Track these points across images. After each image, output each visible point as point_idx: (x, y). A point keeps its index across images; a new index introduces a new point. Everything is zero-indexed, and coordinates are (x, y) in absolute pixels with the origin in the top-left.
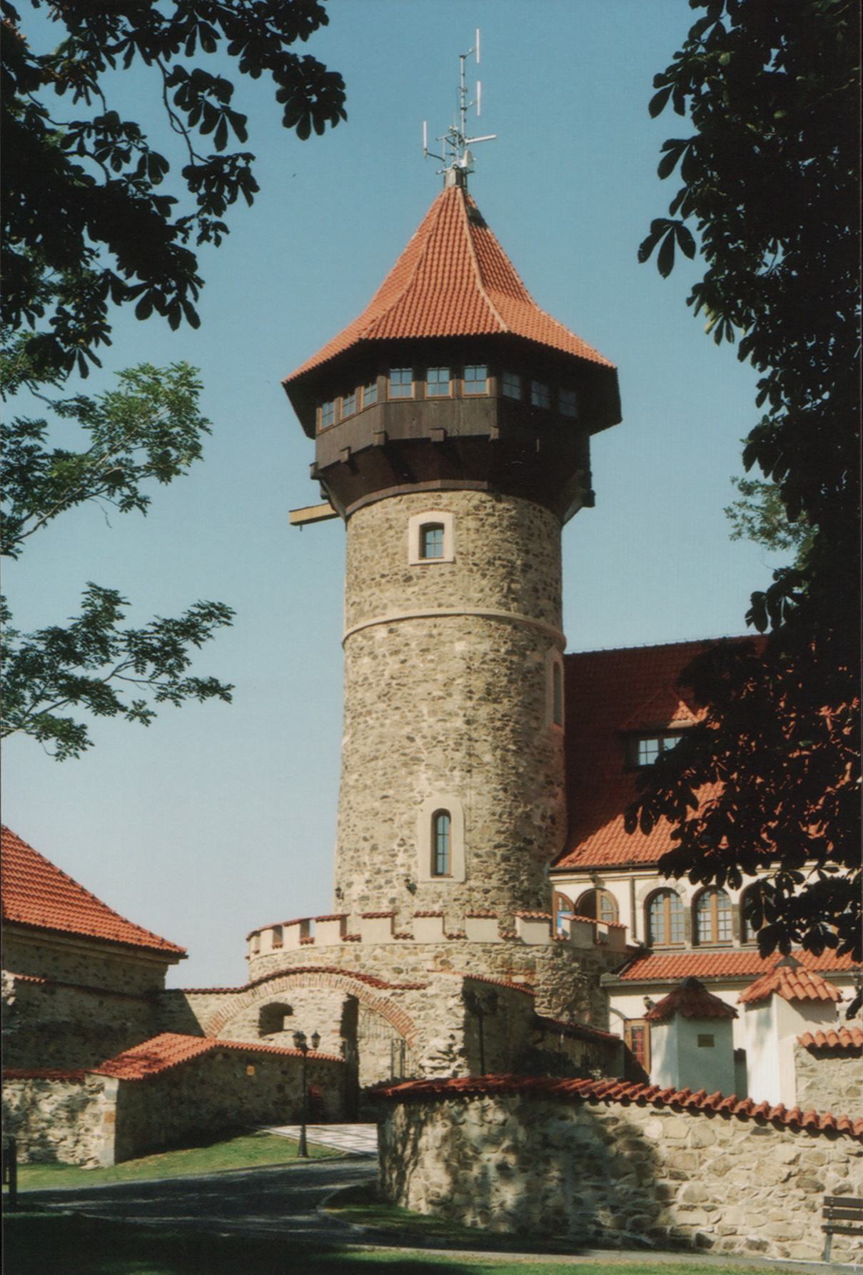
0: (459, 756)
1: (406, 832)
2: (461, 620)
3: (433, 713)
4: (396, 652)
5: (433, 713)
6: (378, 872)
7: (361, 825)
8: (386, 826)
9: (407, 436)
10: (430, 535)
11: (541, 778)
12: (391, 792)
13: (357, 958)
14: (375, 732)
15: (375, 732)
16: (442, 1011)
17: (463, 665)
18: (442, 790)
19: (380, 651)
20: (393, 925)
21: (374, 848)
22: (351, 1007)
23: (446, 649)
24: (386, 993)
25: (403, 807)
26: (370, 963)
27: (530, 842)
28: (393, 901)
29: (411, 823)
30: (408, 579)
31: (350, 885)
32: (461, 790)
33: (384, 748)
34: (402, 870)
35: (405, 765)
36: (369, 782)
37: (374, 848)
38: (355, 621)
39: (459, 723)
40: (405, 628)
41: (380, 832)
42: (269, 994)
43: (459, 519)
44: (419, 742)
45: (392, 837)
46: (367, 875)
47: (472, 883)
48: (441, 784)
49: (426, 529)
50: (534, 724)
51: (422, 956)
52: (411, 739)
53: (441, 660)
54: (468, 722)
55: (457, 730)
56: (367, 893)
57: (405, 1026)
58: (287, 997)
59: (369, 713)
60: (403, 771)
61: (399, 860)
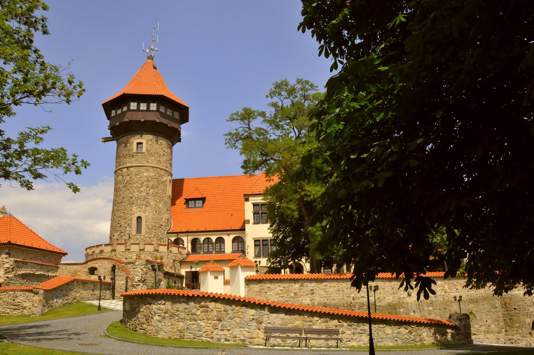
0: (144, 202)
1: (129, 222)
2: (146, 168)
3: (138, 191)
4: (129, 175)
5: (138, 191)
7: (118, 220)
9: (134, 119)
10: (139, 146)
11: (165, 209)
13: (115, 255)
14: (122, 196)
15: (122, 196)
16: (139, 269)
17: (146, 179)
18: (139, 211)
19: (124, 175)
20: (126, 246)
21: (121, 226)
22: (114, 268)
23: (141, 175)
24: (124, 265)
25: (129, 215)
26: (119, 256)
27: (161, 225)
28: (125, 240)
29: (131, 220)
30: (133, 156)
31: (114, 236)
32: (145, 211)
33: (124, 200)
34: (128, 232)
35: (130, 204)
38: (118, 166)
39: (144, 194)
40: (132, 169)
41: (123, 222)
42: (91, 265)
43: (147, 142)
44: (134, 199)
45: (126, 223)
46: (119, 233)
47: (146, 236)
48: (139, 209)
49: (138, 144)
50: (164, 195)
51: (133, 255)
52: (132, 198)
53: (141, 177)
54: (147, 194)
55: (144, 196)
57: (128, 273)
58: (96, 266)
59: (121, 191)
60: (129, 206)
61: (127, 229)
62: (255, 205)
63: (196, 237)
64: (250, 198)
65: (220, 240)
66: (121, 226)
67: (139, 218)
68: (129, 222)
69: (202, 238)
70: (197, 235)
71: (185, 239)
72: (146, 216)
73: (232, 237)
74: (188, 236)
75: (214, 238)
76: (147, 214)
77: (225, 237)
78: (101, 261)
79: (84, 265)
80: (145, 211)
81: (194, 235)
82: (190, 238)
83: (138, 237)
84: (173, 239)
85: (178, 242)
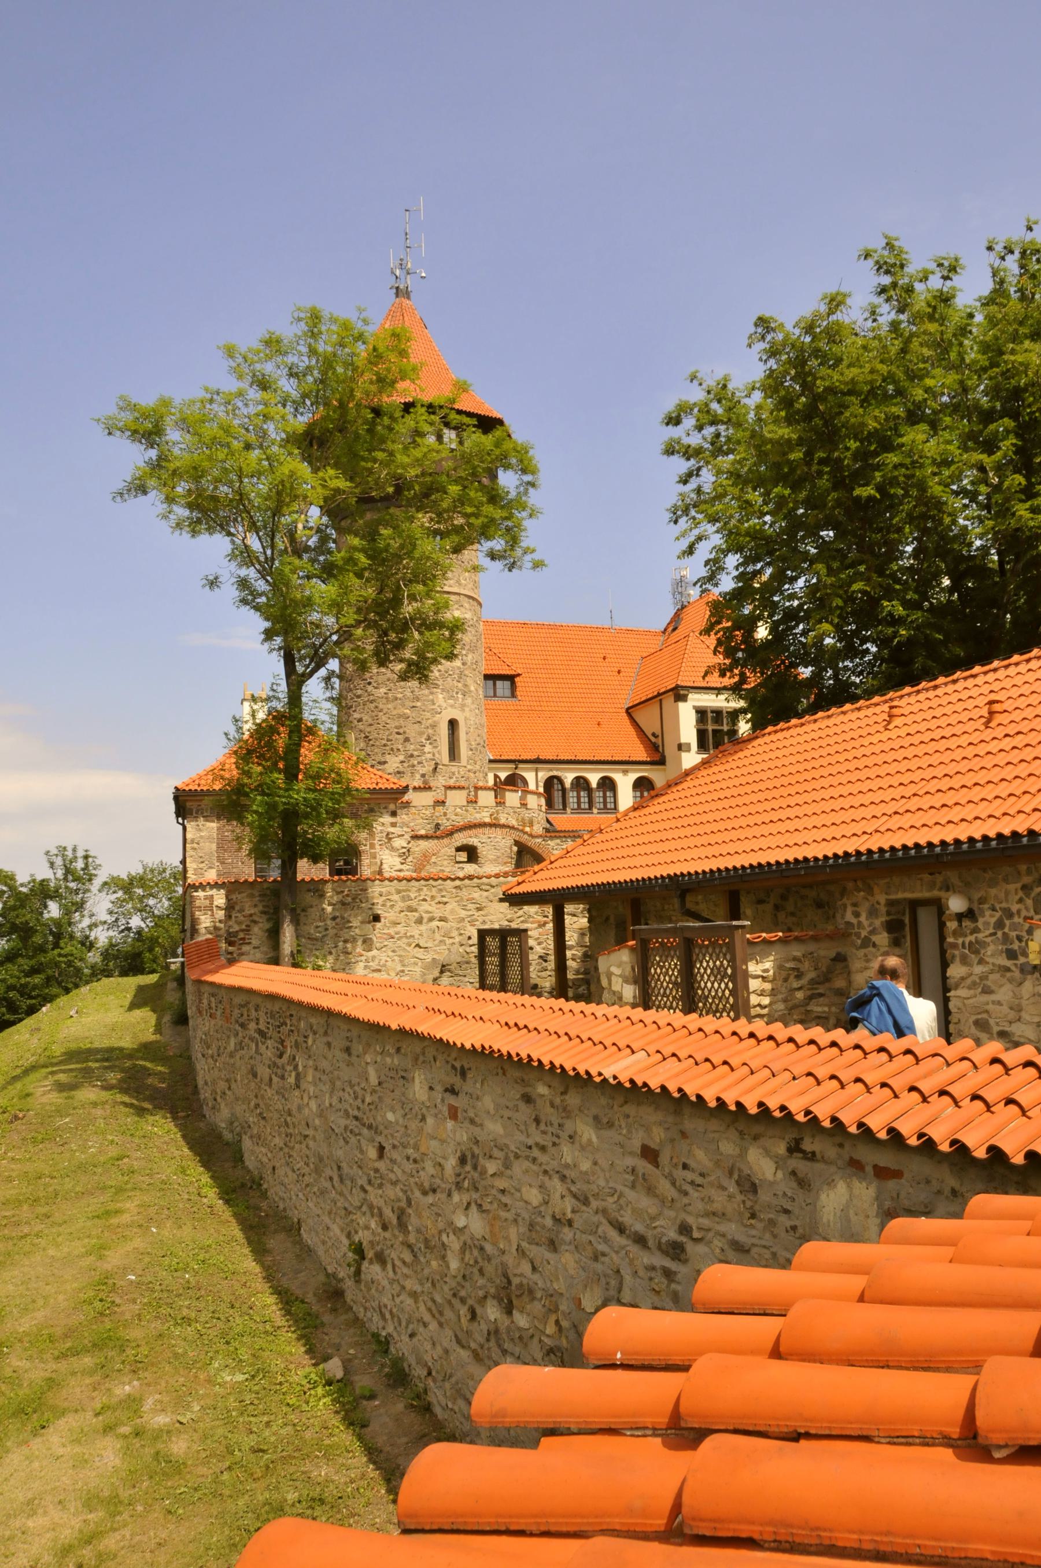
1: (430, 731)
6: (412, 756)
8: (416, 726)
12: (419, 704)
13: (445, 814)
18: (452, 706)
25: (428, 715)
26: (454, 817)
28: (423, 776)
29: (434, 726)
32: (463, 706)
34: (430, 756)
36: (399, 696)
37: (407, 740)
41: (411, 731)
45: (421, 734)
46: (402, 758)
48: (451, 702)
56: (401, 769)
58: (474, 841)
62: (701, 713)
63: (555, 773)
64: (690, 696)
65: (608, 785)
66: (407, 740)
67: (453, 724)
68: (430, 731)
69: (569, 778)
70: (557, 770)
71: (530, 776)
72: (466, 719)
73: (633, 776)
74: (537, 770)
75: (594, 778)
76: (467, 714)
77: (617, 777)
78: (487, 830)
79: (446, 841)
80: (463, 706)
81: (551, 770)
82: (543, 775)
83: (454, 769)
84: (503, 775)
85: (514, 781)
